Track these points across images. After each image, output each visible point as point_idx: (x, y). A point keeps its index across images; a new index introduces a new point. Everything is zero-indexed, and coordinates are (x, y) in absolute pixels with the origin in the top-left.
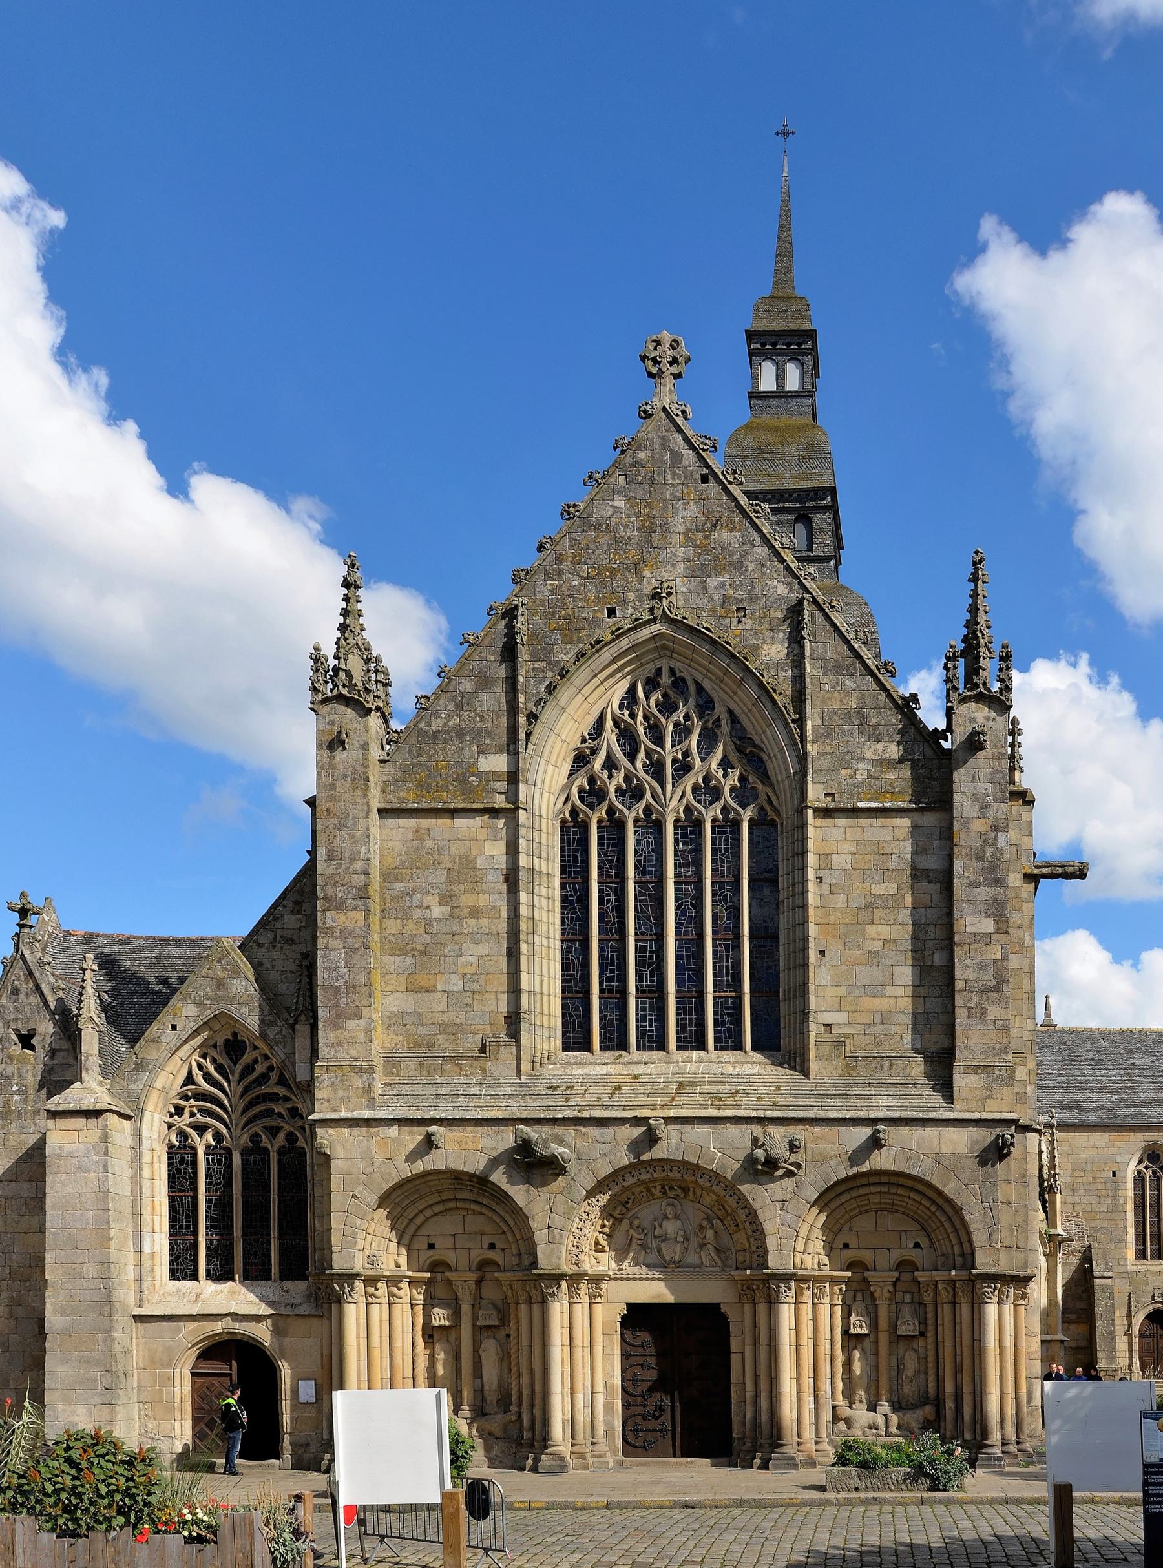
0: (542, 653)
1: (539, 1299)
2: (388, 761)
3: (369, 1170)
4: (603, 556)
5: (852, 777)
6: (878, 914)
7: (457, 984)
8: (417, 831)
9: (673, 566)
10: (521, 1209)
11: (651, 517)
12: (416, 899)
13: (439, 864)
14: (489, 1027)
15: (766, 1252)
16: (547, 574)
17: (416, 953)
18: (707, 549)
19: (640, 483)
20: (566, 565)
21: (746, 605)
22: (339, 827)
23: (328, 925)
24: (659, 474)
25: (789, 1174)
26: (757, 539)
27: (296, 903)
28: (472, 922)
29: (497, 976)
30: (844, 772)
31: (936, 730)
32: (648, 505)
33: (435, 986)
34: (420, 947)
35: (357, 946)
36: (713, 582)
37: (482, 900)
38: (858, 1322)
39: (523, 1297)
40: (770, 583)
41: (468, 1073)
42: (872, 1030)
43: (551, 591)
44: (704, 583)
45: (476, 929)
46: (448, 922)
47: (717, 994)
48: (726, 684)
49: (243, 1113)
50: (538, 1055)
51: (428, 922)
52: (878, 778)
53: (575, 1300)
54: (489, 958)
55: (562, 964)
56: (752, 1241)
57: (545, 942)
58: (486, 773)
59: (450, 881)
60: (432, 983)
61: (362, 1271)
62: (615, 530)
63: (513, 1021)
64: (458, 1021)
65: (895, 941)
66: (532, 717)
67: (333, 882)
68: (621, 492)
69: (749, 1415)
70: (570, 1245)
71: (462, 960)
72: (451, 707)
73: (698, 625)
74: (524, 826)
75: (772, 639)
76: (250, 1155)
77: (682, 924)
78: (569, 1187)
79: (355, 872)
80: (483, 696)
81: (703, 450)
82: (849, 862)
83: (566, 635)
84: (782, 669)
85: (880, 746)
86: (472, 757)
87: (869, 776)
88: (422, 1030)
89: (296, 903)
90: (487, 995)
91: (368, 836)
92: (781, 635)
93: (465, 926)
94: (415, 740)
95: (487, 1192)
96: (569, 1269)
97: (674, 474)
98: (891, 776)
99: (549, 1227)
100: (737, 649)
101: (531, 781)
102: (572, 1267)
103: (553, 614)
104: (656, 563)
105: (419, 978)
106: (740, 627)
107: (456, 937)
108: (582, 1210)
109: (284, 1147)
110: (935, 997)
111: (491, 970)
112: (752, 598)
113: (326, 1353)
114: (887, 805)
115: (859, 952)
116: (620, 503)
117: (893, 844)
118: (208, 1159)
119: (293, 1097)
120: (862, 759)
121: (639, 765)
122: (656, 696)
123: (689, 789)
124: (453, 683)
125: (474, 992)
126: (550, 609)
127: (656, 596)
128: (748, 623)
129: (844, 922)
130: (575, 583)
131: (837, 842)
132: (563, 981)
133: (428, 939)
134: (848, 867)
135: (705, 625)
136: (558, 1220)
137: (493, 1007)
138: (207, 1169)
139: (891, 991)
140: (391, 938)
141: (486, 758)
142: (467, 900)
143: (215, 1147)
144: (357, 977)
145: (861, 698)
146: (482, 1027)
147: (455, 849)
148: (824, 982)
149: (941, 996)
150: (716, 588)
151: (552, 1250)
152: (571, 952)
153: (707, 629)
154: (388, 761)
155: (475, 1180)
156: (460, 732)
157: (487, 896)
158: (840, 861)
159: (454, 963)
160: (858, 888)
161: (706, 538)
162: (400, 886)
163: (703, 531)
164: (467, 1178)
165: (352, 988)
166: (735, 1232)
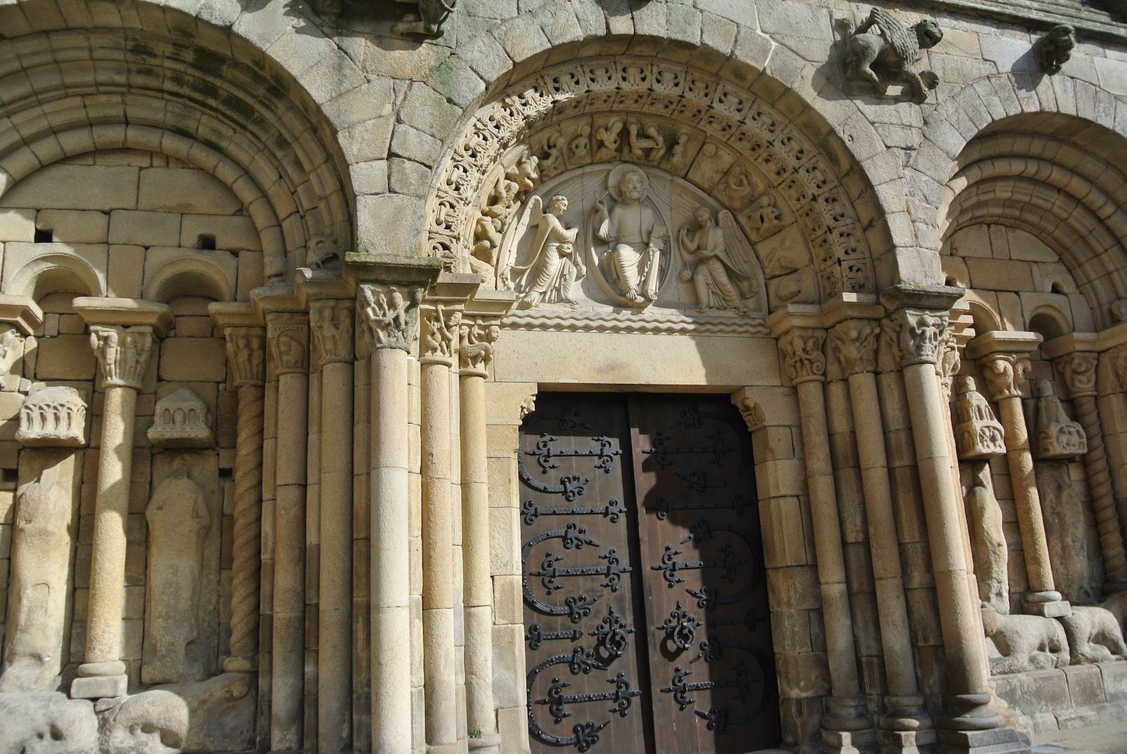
10: (318, 107)
25: (914, 94)
78: (442, 69)
99: (391, 155)
108: (460, 143)
136: (414, 142)
155: (189, 56)
164: (169, 50)
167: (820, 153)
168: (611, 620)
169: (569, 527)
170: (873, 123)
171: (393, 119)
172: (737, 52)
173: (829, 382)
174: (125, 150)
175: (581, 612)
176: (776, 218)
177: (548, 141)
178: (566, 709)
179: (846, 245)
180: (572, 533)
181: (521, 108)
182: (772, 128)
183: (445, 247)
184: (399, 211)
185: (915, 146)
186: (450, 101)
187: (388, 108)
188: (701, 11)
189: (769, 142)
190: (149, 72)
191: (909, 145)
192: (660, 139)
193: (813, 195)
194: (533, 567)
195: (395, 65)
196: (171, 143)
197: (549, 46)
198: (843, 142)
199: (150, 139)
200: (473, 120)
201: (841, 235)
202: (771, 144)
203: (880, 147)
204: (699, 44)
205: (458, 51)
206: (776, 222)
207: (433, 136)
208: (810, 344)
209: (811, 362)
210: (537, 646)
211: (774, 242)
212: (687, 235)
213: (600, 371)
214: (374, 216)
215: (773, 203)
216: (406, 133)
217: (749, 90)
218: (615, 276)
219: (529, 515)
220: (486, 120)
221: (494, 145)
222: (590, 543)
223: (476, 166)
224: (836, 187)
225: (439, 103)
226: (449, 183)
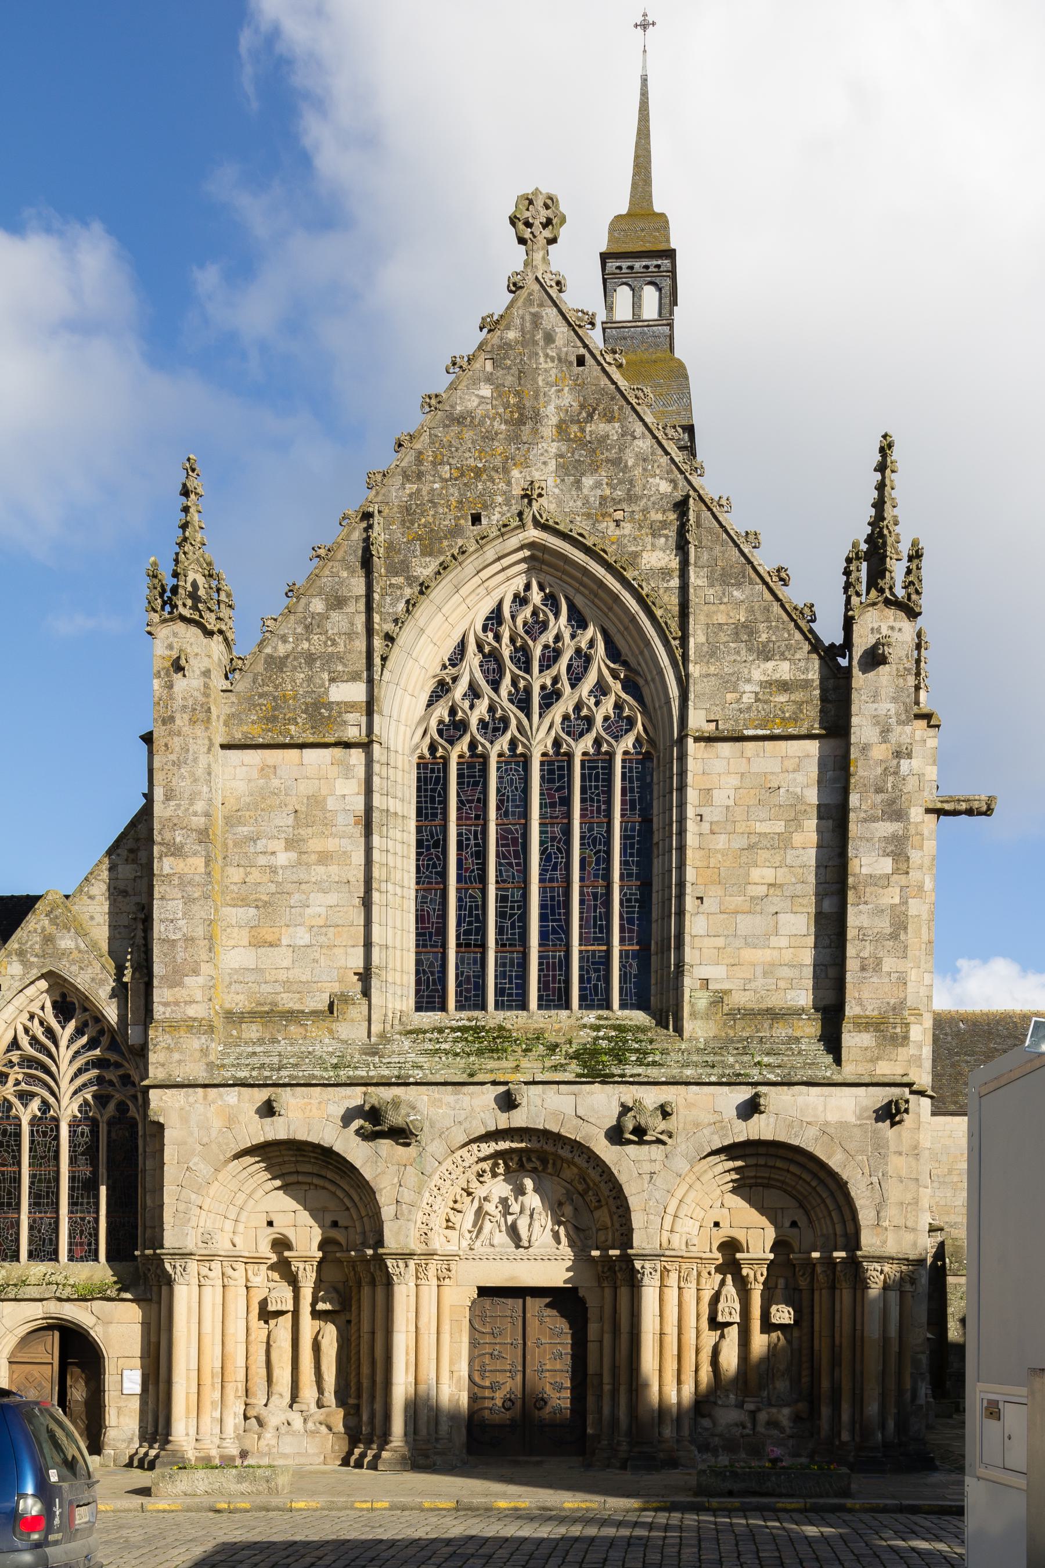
0: (401, 568)
1: (384, 1281)
2: (231, 691)
3: (205, 1140)
4: (467, 455)
5: (738, 701)
6: (763, 855)
7: (303, 937)
8: (262, 769)
9: (545, 463)
11: (520, 407)
12: (260, 845)
13: (286, 805)
14: (337, 984)
15: (631, 1230)
16: (406, 477)
17: (260, 904)
18: (582, 443)
19: (509, 368)
20: (427, 466)
21: (625, 506)
22: (177, 764)
23: (165, 873)
24: (530, 358)
26: (639, 429)
27: (131, 851)
28: (321, 869)
29: (346, 929)
30: (730, 697)
31: (833, 645)
32: (518, 394)
33: (279, 940)
34: (265, 898)
35: (196, 895)
36: (588, 481)
37: (331, 844)
38: (727, 1310)
39: (365, 1280)
40: (651, 480)
41: (314, 1034)
42: (753, 985)
43: (410, 495)
44: (578, 484)
45: (325, 877)
46: (295, 869)
47: (583, 948)
48: (601, 599)
49: (72, 1080)
50: (390, 1015)
51: (273, 869)
52: (766, 702)
54: (338, 909)
55: (417, 916)
56: (615, 1217)
57: (399, 890)
58: (338, 703)
59: (297, 825)
60: (277, 936)
61: (194, 1250)
62: (482, 423)
63: (365, 977)
64: (304, 979)
65: (781, 886)
66: (390, 638)
67: (171, 824)
68: (489, 379)
69: (606, 1410)
70: (419, 1222)
71: (308, 911)
72: (300, 630)
73: (571, 531)
74: (378, 762)
75: (653, 545)
76: (78, 1126)
77: (547, 871)
79: (195, 814)
80: (335, 615)
81: (580, 326)
82: (732, 797)
83: (426, 547)
84: (663, 579)
85: (770, 665)
86: (322, 685)
87: (757, 700)
88: (266, 989)
89: (131, 851)
90: (336, 950)
91: (209, 774)
92: (663, 540)
93: (313, 874)
94: (260, 668)
95: (331, 1164)
96: (418, 1248)
97: (547, 356)
98: (783, 698)
100: (614, 558)
101: (386, 711)
102: (420, 1245)
103: (412, 523)
104: (526, 464)
105: (263, 931)
106: (618, 533)
107: (303, 886)
109: (114, 1117)
110: (824, 947)
111: (340, 922)
112: (631, 498)
113: (153, 1339)
114: (777, 731)
115: (740, 899)
116: (486, 391)
117: (782, 776)
118: (32, 1131)
119: (125, 1064)
120: (749, 681)
121: (504, 692)
122: (527, 612)
123: (558, 720)
124: (303, 601)
125: (321, 947)
126: (409, 513)
127: (527, 497)
128: (627, 528)
129: (725, 864)
130: (436, 486)
131: (719, 775)
132: (417, 935)
133: (273, 888)
134: (731, 803)
135: (580, 531)
136: (407, 1196)
137: (342, 963)
138: (32, 1142)
139: (774, 941)
140: (232, 887)
141: (338, 687)
142: (315, 845)
143: (41, 1118)
144: (197, 929)
145: (751, 610)
146: (330, 984)
147: (304, 788)
148: (702, 932)
149: (830, 947)
150: (592, 489)
152: (426, 903)
153: (581, 535)
154: (231, 691)
156: (310, 659)
157: (337, 840)
158: (720, 797)
159: (300, 915)
160: (741, 827)
161: (582, 430)
162: (244, 830)
163: (579, 422)
165: (189, 940)
166: (597, 1208)
174: (298, 1183)
187: (396, 1180)
190: (304, 1156)
192: (538, 1163)
196: (316, 1181)
199: (308, 1180)
208: (606, 1269)
213: (506, 1280)
221: (449, 1182)
225: (417, 1175)
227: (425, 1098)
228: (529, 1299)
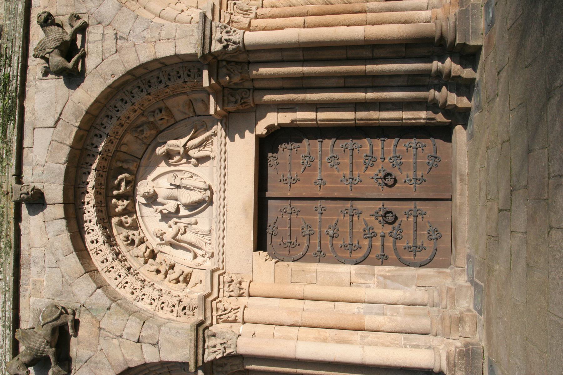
53: (239, 314)
151: (168, 341)
167: (122, 89)
168: (375, 215)
169: (328, 234)
170: (103, 60)
171: (121, 339)
172: (68, 143)
173: (254, 86)
175: (371, 231)
176: (161, 112)
177: (125, 241)
178: (419, 244)
179: (175, 77)
180: (331, 232)
181: (109, 262)
182: (110, 117)
183: (184, 308)
184: (168, 341)
185: (115, 32)
186: (108, 309)
188: (46, 162)
189: (118, 119)
191: (114, 37)
193: (147, 95)
194: (347, 255)
195: (92, 336)
197: (74, 253)
198: (116, 81)
200: (117, 289)
201: (169, 79)
202: (119, 118)
203: (116, 56)
204: (65, 166)
205: (82, 303)
206: (163, 112)
207: (128, 320)
208: (232, 99)
209: (242, 98)
210: (386, 257)
211: (175, 111)
212: (173, 159)
214: (171, 353)
215: (152, 114)
216: (127, 334)
217: (88, 131)
218: (196, 204)
219: (321, 258)
220: (117, 282)
221: (130, 279)
222: (336, 224)
223: (141, 289)
224: (141, 81)
226: (151, 304)
227: (33, 299)
228: (268, 195)
